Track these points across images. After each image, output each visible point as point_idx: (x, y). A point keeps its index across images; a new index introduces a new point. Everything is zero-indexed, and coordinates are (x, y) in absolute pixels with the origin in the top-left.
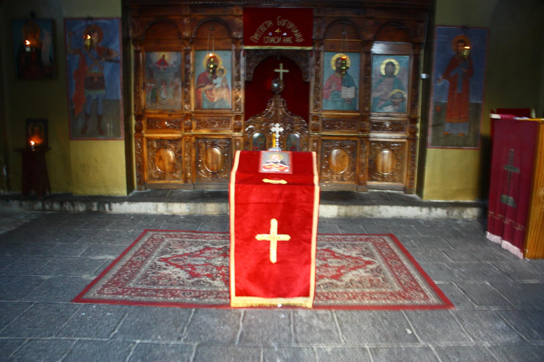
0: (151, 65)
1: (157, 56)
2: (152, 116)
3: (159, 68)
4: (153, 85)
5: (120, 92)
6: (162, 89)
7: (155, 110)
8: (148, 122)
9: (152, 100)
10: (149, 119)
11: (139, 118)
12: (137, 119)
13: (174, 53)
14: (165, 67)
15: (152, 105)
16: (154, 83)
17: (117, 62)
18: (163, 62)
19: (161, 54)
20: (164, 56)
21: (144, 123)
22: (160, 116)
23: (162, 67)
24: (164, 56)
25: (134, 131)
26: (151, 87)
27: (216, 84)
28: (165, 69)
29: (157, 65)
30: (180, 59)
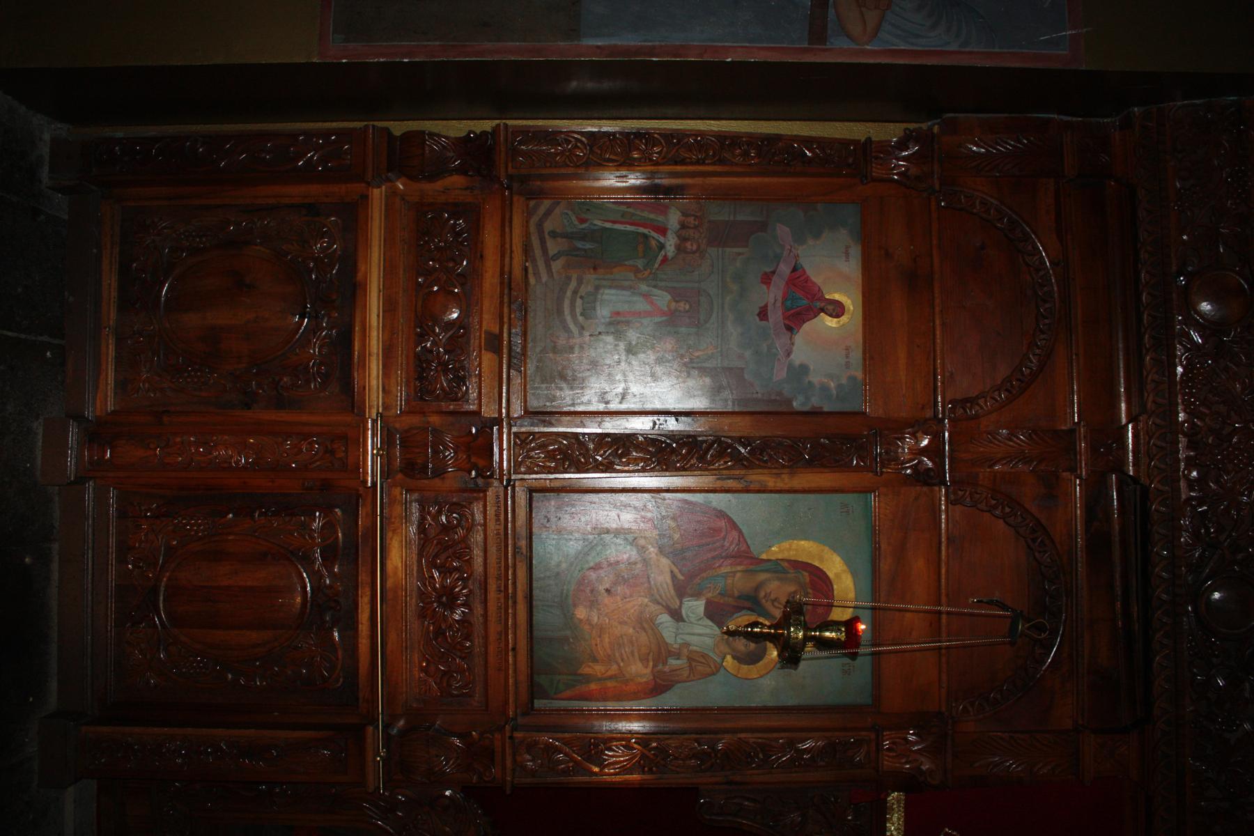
0: (783, 231)
1: (838, 274)
2: (490, 238)
3: (767, 279)
4: (671, 243)
5: (629, 40)
6: (646, 296)
7: (527, 250)
8: (457, 210)
9: (583, 236)
10: (473, 214)
11: (477, 154)
12: (465, 143)
13: (859, 374)
14: (776, 316)
15: (554, 234)
16: (679, 249)
17: (818, 34)
18: (804, 304)
19: (850, 300)
20: (837, 310)
21: (454, 184)
22: (490, 279)
23: (773, 295)
24: (837, 310)
25: (398, 128)
26: (663, 231)
27: (677, 615)
28: (763, 314)
29: (785, 269)
30: (815, 401)
